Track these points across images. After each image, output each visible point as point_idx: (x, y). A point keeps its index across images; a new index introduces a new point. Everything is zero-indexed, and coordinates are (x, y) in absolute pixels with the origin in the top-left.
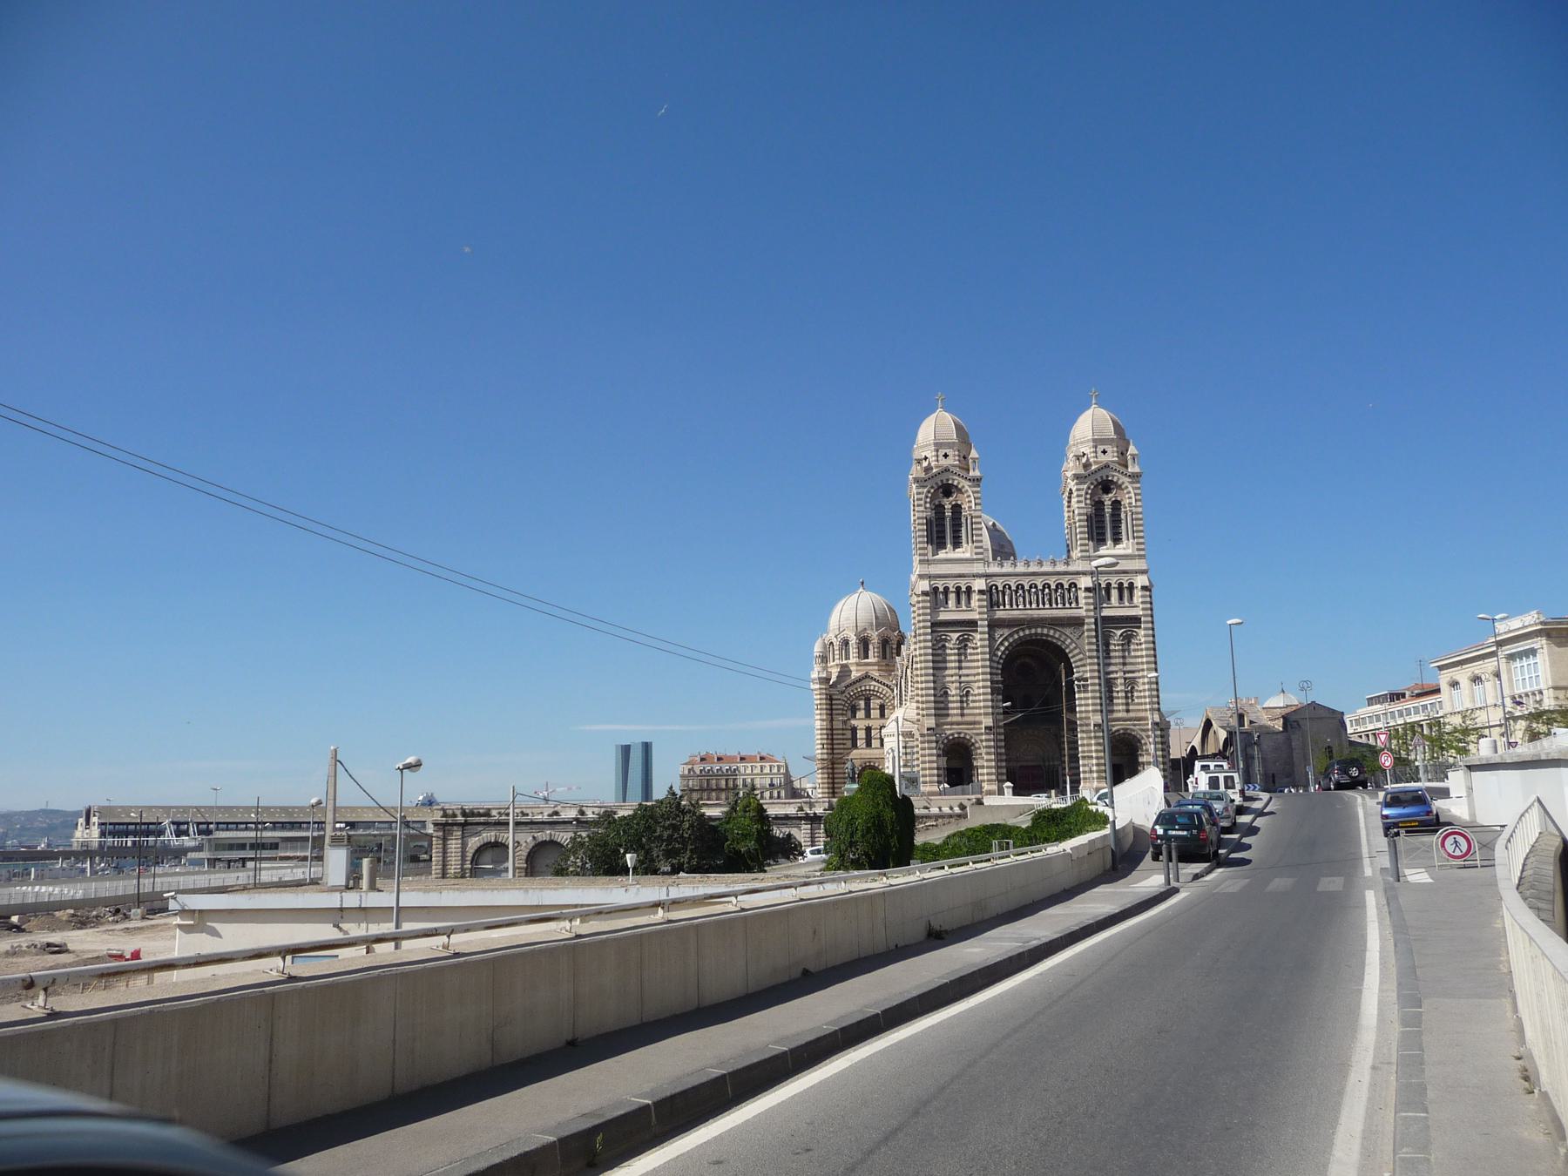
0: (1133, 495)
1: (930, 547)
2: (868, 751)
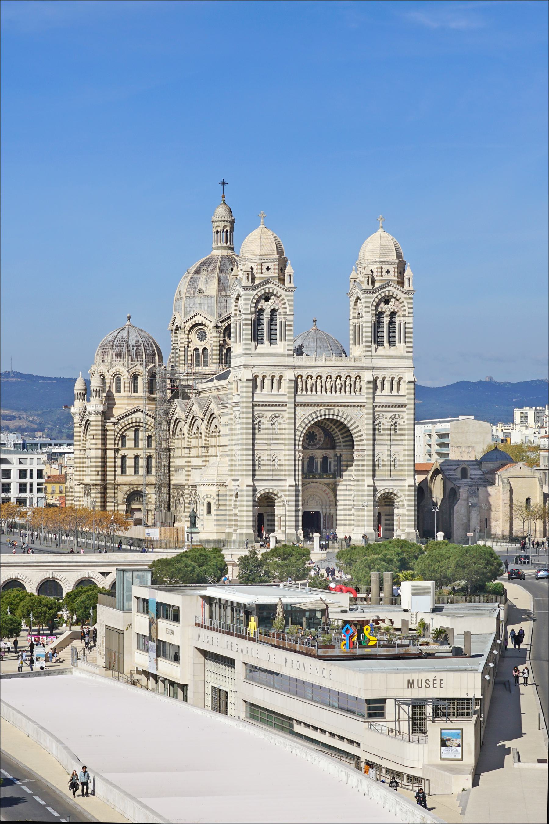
0: (406, 308)
1: (253, 343)
2: (136, 478)
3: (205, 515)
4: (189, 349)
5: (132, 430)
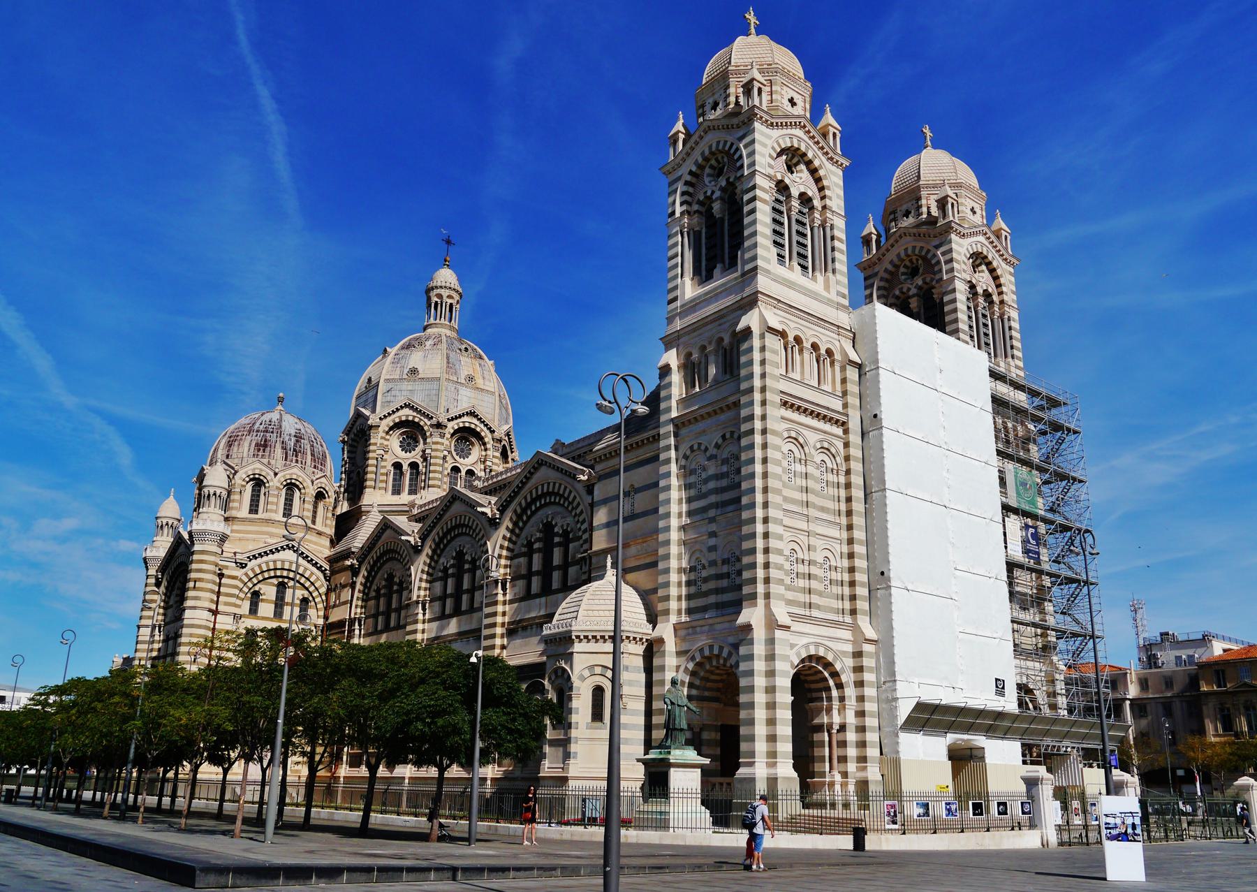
3: (582, 725)
4: (383, 464)
5: (274, 585)
